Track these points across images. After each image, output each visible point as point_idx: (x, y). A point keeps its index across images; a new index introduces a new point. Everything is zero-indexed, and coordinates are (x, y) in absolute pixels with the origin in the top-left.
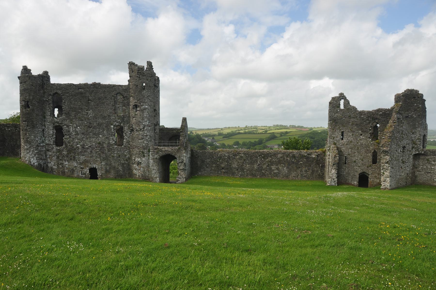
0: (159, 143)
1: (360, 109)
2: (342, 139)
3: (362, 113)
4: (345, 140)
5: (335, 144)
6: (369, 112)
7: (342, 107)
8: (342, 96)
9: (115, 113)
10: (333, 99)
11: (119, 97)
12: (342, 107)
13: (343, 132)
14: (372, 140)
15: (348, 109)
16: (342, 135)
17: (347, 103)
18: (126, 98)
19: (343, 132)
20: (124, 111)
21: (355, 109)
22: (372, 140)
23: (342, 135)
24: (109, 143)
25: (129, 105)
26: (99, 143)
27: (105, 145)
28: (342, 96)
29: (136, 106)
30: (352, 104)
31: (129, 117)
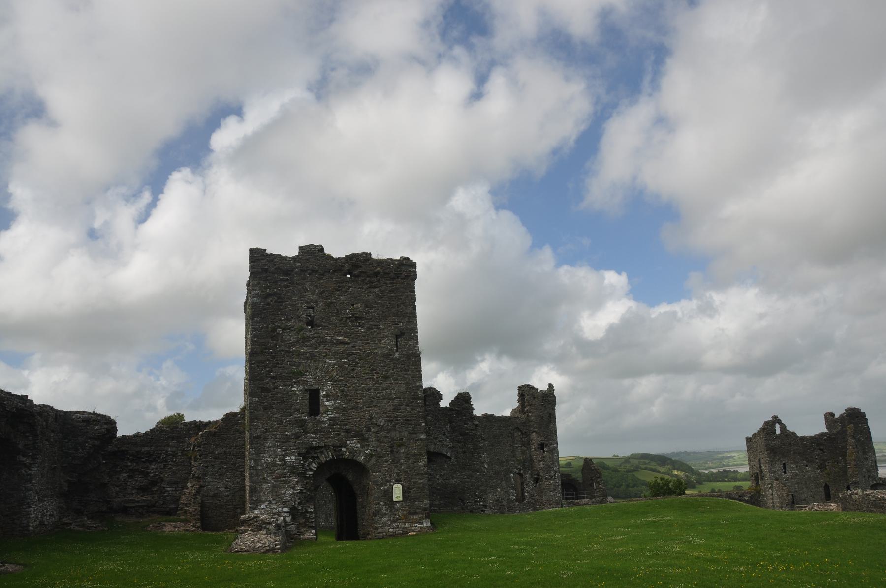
0: (567, 495)
1: (800, 434)
2: (785, 472)
3: (804, 438)
4: (788, 474)
5: (777, 479)
6: (811, 437)
7: (778, 432)
8: (776, 420)
9: (514, 456)
10: (767, 423)
11: (516, 434)
12: (778, 432)
13: (784, 464)
14: (821, 471)
15: (787, 435)
16: (784, 468)
17: (783, 427)
18: (527, 434)
19: (784, 464)
20: (523, 453)
21: (794, 434)
22: (821, 471)
23: (784, 468)
24: (509, 499)
25: (528, 444)
26: (497, 500)
27: (504, 503)
28: (776, 420)
29: (542, 446)
30: (790, 428)
31: (531, 460)
